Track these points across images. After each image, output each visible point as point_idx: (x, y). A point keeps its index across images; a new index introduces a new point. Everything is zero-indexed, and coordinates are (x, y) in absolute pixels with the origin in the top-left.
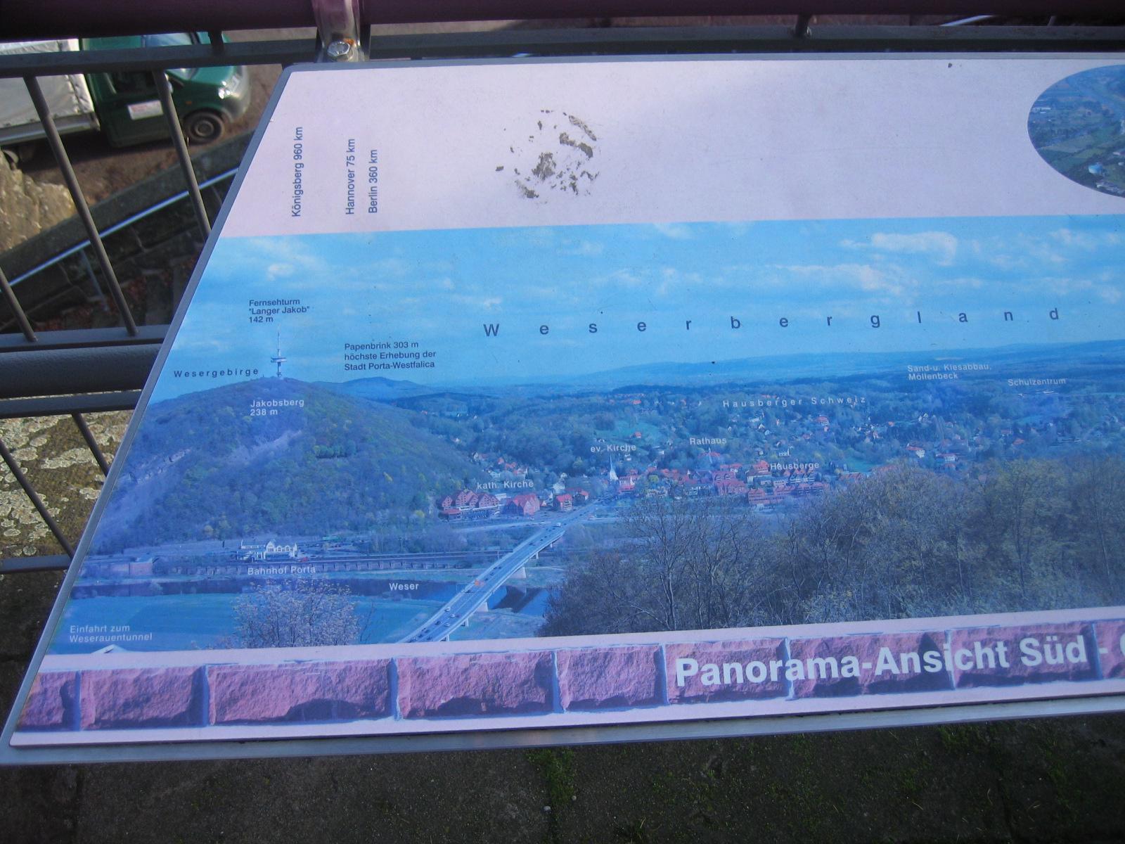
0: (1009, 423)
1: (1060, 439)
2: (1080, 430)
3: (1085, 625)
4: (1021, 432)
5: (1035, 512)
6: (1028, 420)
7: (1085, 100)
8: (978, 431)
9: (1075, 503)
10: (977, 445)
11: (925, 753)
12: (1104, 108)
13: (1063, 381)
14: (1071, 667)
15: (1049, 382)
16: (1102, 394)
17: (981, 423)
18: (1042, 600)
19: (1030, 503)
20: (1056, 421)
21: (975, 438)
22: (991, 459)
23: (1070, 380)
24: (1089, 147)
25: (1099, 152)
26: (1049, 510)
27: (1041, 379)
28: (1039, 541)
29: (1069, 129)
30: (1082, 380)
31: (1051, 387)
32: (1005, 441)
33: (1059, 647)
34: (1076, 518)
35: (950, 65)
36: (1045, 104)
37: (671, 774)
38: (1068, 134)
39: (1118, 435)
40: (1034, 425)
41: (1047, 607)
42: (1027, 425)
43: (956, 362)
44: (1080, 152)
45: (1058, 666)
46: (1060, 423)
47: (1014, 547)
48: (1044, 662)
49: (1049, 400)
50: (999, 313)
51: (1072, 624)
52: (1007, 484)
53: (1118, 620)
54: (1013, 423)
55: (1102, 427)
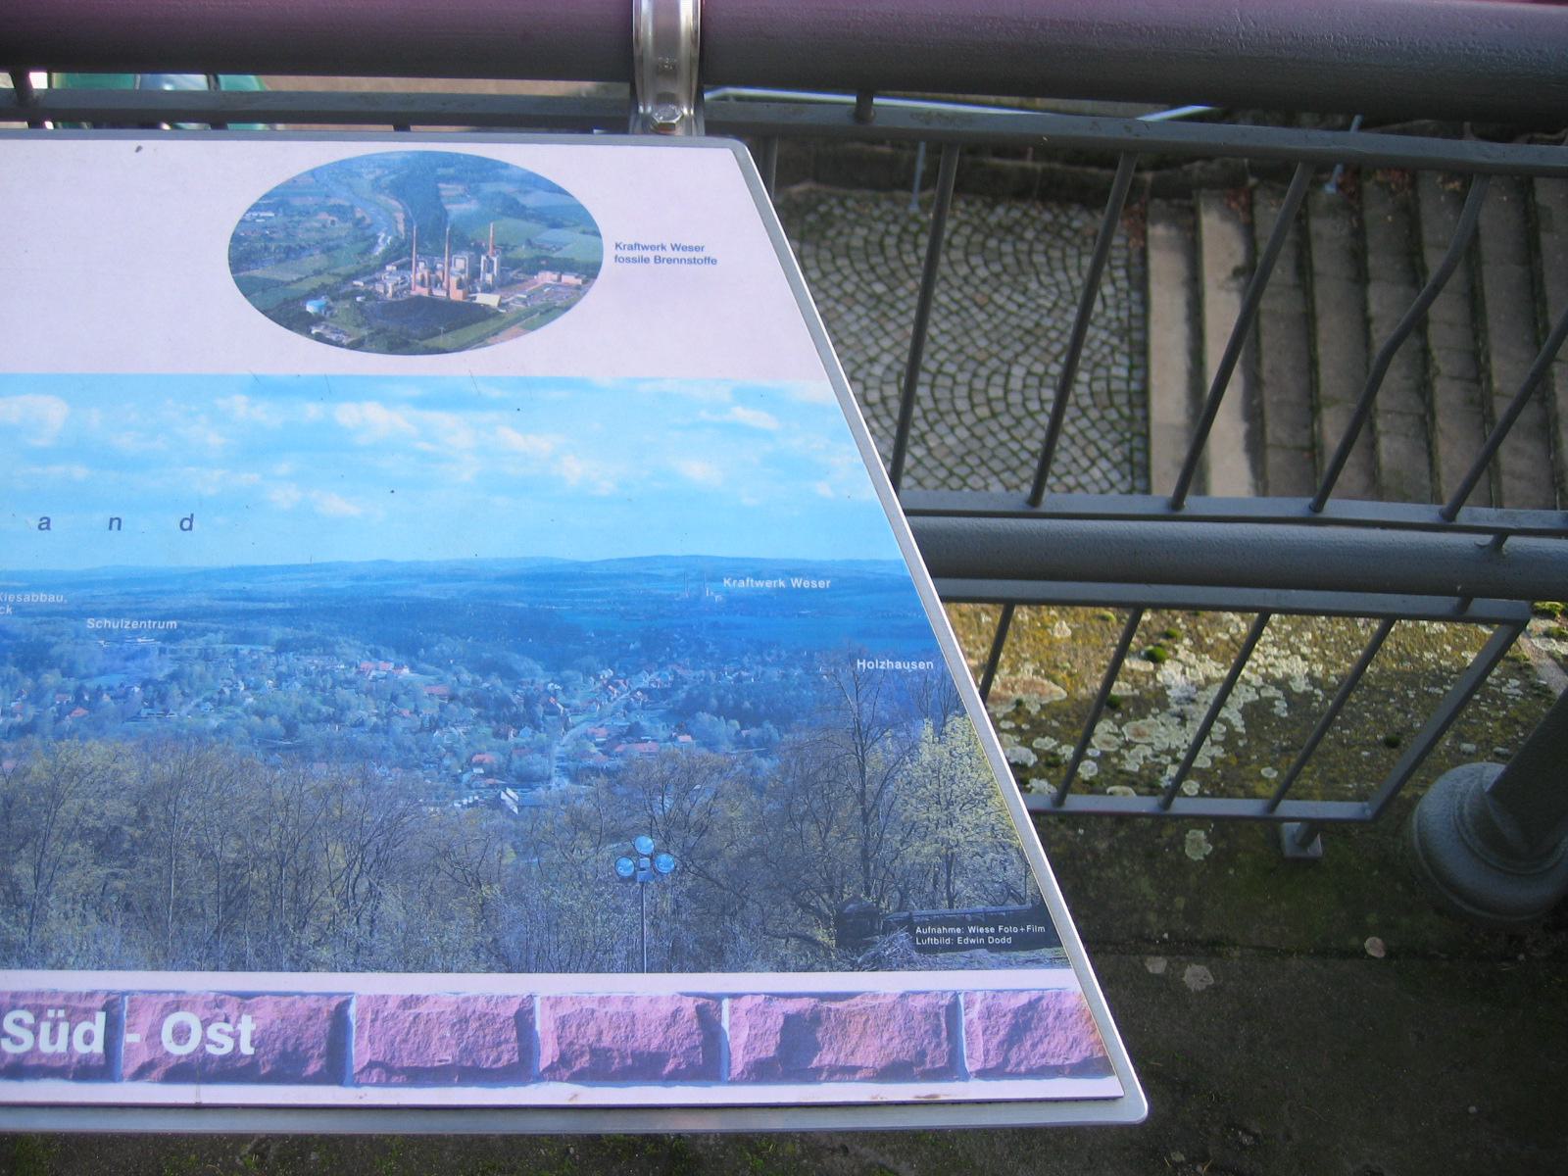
0: (72, 684)
1: (144, 712)
2: (180, 699)
3: (112, 997)
4: (86, 698)
5: (77, 821)
6: (103, 681)
7: (332, 201)
8: (20, 694)
9: (142, 811)
10: (14, 715)
11: (572, 1150)
12: (358, 215)
13: (173, 624)
14: (74, 1060)
15: (150, 624)
16: (230, 646)
17: (29, 682)
18: (54, 954)
19: (73, 805)
20: (144, 685)
21: (13, 704)
22: (29, 736)
23: (185, 623)
24: (318, 273)
25: (329, 280)
26: (100, 819)
27: (139, 620)
28: (72, 865)
29: (293, 245)
30: (202, 624)
31: (150, 633)
32: (59, 711)
33: (64, 1028)
34: (138, 833)
35: (139, 149)
36: (268, 208)
37: (193, 1157)
38: (291, 253)
39: (238, 711)
40: (110, 688)
41: (60, 965)
42: (99, 688)
43: (16, 590)
44: (300, 280)
45: (55, 1055)
46: (150, 687)
47: (31, 871)
48: (35, 1049)
49: (144, 652)
50: (101, 518)
51: (91, 995)
52: (45, 775)
53: (168, 992)
54: (78, 683)
55: (216, 696)
